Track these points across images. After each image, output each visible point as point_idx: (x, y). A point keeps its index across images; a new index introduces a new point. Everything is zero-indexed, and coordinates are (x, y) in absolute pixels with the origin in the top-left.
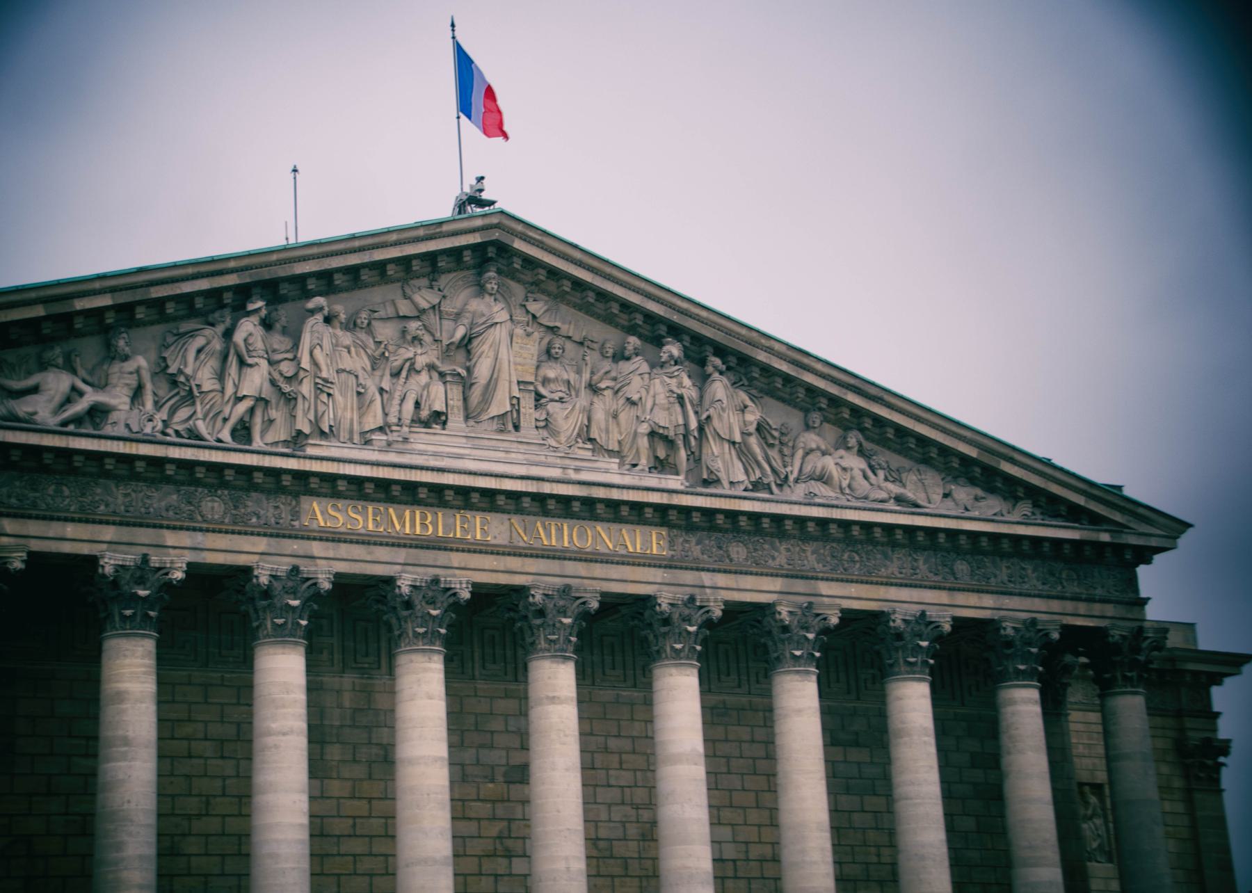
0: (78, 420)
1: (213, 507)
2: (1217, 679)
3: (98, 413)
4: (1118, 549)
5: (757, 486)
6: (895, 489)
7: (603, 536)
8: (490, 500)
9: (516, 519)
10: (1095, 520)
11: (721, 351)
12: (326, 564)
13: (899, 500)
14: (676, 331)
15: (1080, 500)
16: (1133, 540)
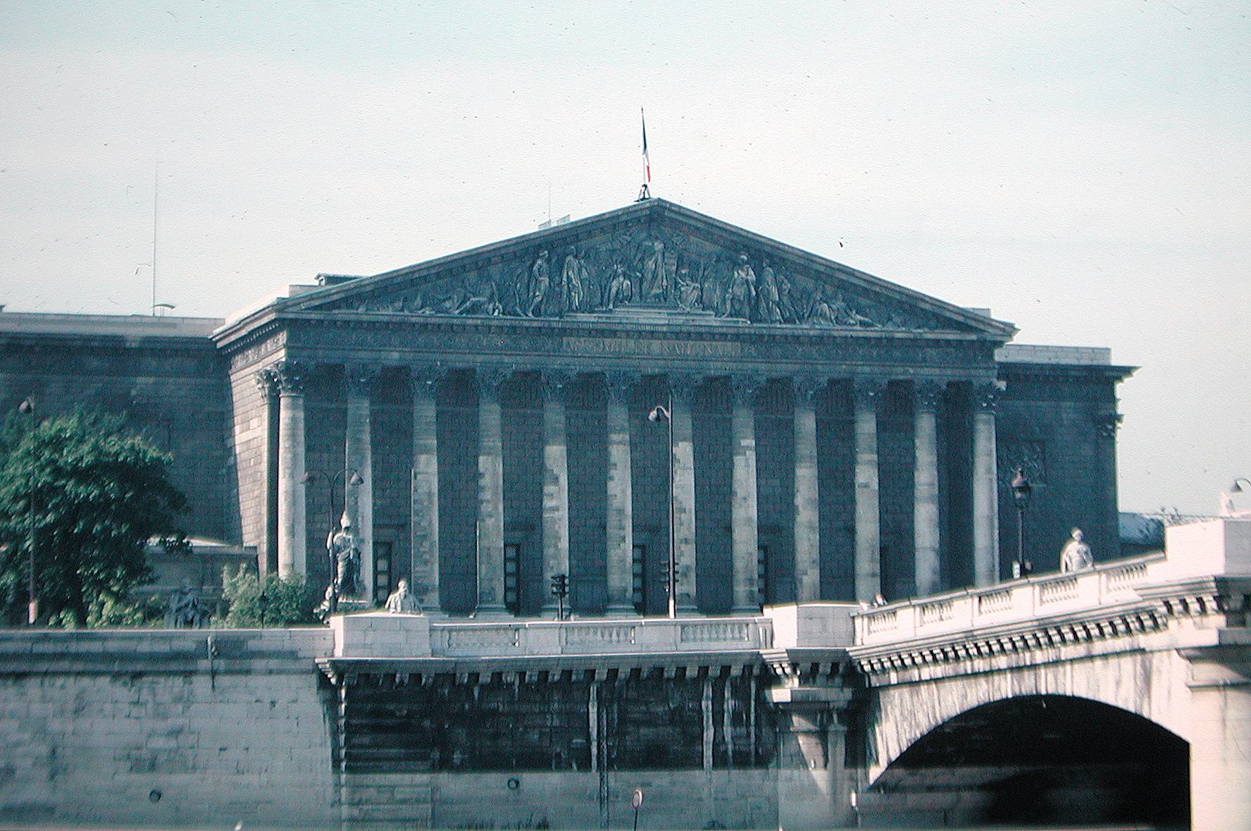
0: (467, 311)
1: (525, 344)
2: (1120, 379)
3: (475, 309)
4: (982, 342)
5: (786, 321)
6: (859, 317)
7: (708, 348)
8: (652, 334)
9: (665, 342)
10: (971, 329)
11: (769, 256)
12: (577, 367)
13: (862, 323)
14: (747, 248)
15: (961, 319)
16: (989, 338)
